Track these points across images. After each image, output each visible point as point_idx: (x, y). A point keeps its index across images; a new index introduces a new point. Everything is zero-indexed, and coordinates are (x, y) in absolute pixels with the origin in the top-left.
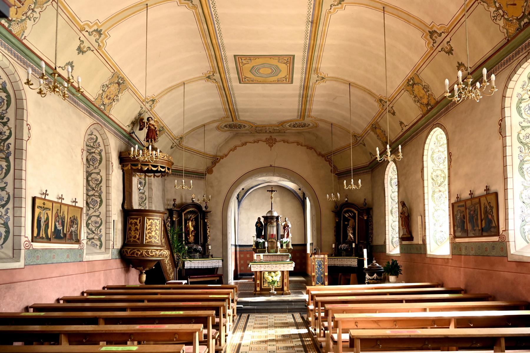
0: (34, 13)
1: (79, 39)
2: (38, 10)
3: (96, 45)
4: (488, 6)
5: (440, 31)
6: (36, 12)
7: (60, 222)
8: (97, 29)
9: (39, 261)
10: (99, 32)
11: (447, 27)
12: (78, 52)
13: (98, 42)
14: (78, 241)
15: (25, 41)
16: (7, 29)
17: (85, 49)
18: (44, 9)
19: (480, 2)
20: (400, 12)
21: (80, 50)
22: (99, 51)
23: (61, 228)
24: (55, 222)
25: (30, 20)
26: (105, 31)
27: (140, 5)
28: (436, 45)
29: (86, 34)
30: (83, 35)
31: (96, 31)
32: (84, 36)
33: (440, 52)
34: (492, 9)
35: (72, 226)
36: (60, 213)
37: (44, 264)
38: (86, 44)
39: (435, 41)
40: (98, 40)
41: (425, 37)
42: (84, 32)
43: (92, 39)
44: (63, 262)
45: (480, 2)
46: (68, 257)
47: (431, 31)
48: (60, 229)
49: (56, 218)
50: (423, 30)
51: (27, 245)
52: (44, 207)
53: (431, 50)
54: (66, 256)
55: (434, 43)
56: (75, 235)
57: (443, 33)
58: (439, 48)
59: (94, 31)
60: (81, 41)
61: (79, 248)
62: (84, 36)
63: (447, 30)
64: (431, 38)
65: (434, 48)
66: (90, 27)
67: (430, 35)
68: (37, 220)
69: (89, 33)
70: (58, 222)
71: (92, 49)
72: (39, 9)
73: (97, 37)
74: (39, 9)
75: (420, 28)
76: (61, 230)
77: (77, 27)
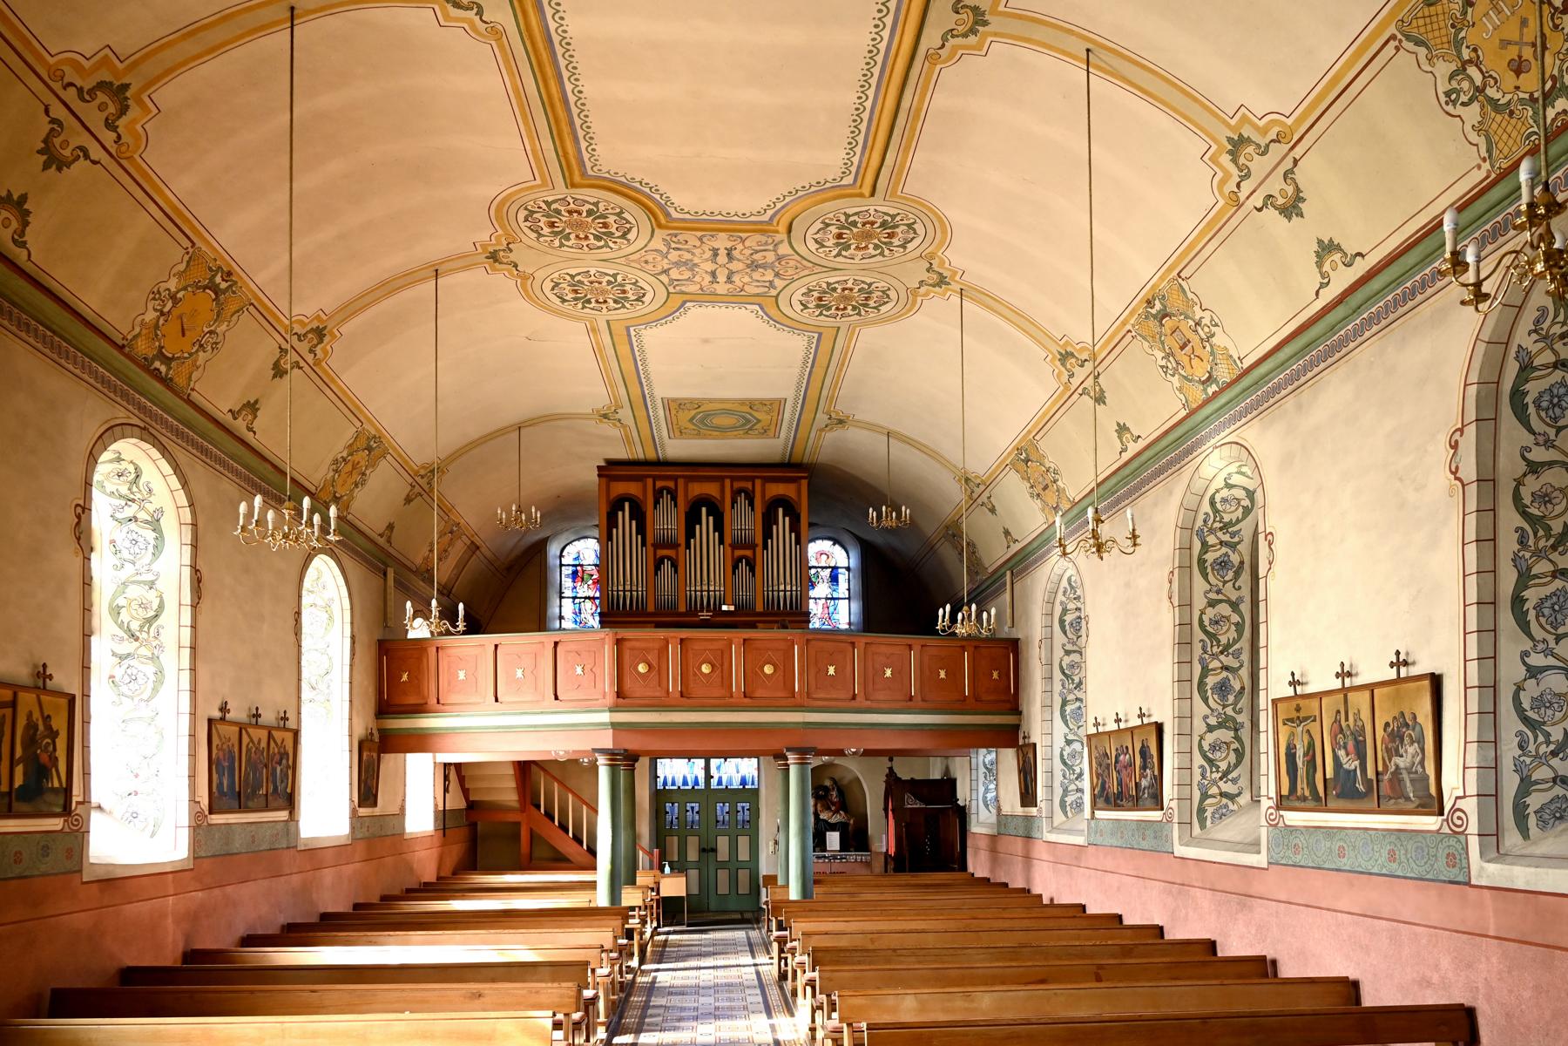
0: (1204, 322)
1: (1259, 210)
2: (1198, 314)
3: (1277, 150)
4: (180, 274)
5: (126, 127)
6: (1201, 318)
7: (1351, 744)
8: (1230, 152)
9: (1299, 857)
10: (1238, 145)
11: (136, 156)
12: (1297, 215)
13: (1267, 146)
14: (1434, 804)
15: (1247, 363)
16: (1222, 390)
17: (1290, 190)
18: (1196, 299)
19: (188, 253)
20: (240, 32)
21: (1292, 209)
22: (1296, 138)
23: (1357, 763)
24: (1334, 751)
25: (1213, 335)
26: (1228, 125)
27: (1104, 65)
28: (70, 95)
29: (1247, 187)
30: (1248, 198)
31: (1234, 155)
32: (1252, 194)
33: (47, 112)
34: (173, 285)
35: (1397, 750)
36: (1347, 719)
37: (1313, 868)
38: (1276, 185)
39: (87, 97)
40: (1259, 146)
41: (105, 62)
42: (1242, 196)
43: (1259, 165)
44: (1375, 870)
45: (188, 253)
46: (1392, 857)
47: (128, 94)
48: (1353, 767)
49: (1336, 736)
50: (135, 64)
51: (1272, 817)
52: (1298, 717)
53: (49, 67)
54: (1385, 854)
55: (80, 90)
56: (1412, 781)
57: (114, 135)
58: (59, 111)
59: (1235, 161)
60: (1265, 205)
61: (1446, 830)
62: (1252, 194)
63: (128, 154)
64: (102, 86)
65: (57, 86)
66: (1227, 176)
67: (111, 83)
68: (1286, 754)
69: (1243, 178)
70: (1345, 748)
71: (1290, 165)
72: (1197, 308)
73: (1250, 149)
74: (1197, 308)
75: (147, 56)
76: (1355, 769)
77: (1231, 217)
